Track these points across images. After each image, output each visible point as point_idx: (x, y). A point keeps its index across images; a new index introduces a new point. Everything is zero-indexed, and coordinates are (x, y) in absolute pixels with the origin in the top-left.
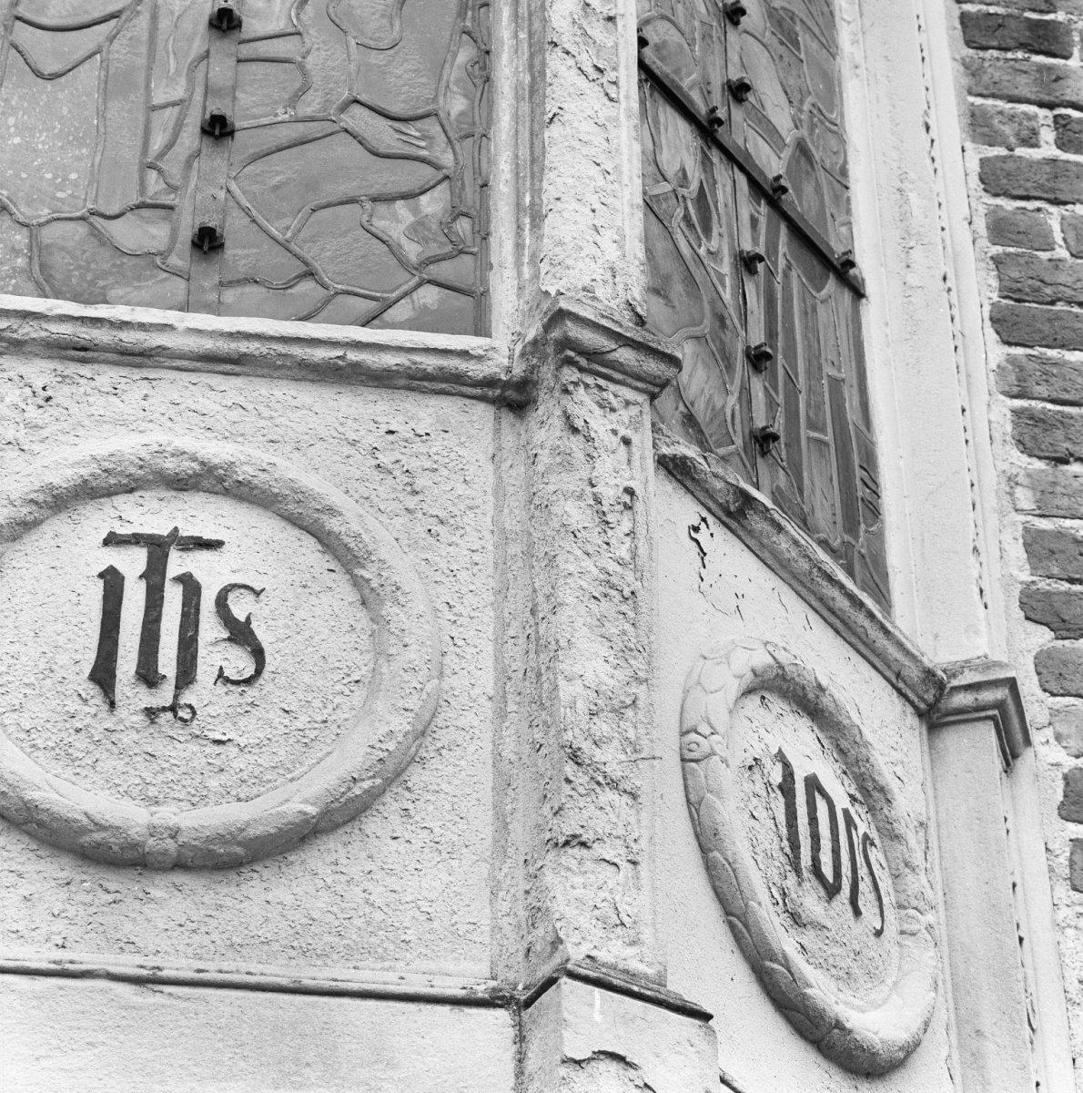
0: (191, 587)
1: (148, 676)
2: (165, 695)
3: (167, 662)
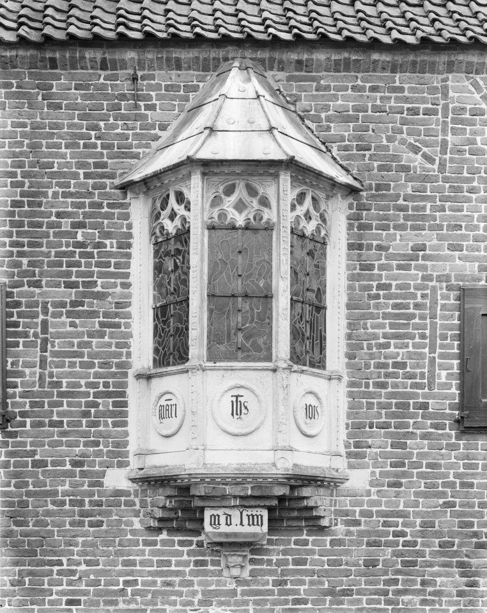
0: (240, 401)
1: (237, 414)
2: (239, 416)
3: (239, 413)
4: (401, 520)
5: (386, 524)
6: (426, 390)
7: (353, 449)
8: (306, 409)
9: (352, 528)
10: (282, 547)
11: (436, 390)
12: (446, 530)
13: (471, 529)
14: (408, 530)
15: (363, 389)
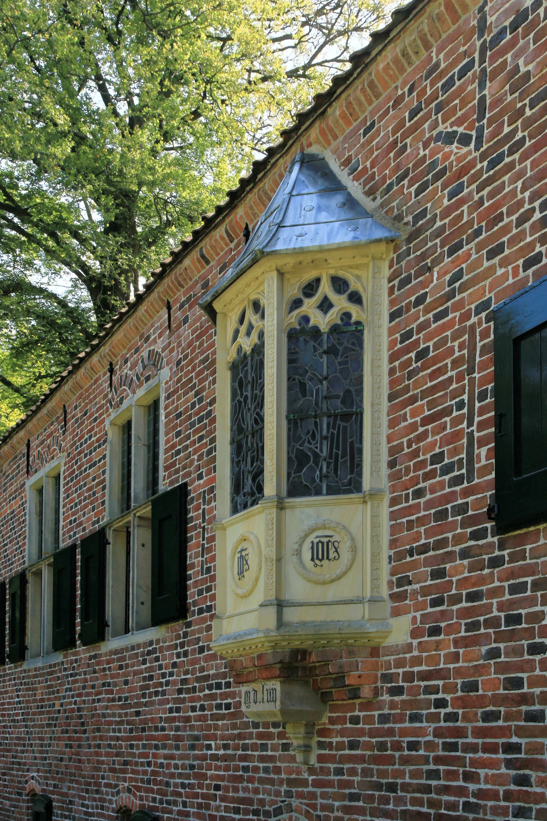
4: (441, 683)
5: (429, 690)
6: (465, 484)
7: (396, 590)
8: (312, 548)
9: (396, 698)
10: (339, 727)
11: (476, 481)
12: (490, 693)
13: (520, 691)
14: (448, 697)
15: (404, 505)
